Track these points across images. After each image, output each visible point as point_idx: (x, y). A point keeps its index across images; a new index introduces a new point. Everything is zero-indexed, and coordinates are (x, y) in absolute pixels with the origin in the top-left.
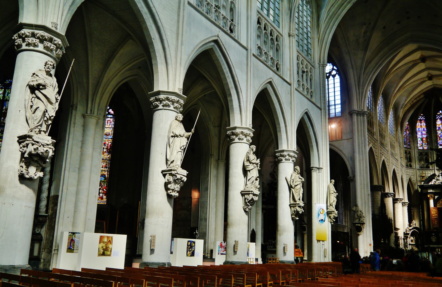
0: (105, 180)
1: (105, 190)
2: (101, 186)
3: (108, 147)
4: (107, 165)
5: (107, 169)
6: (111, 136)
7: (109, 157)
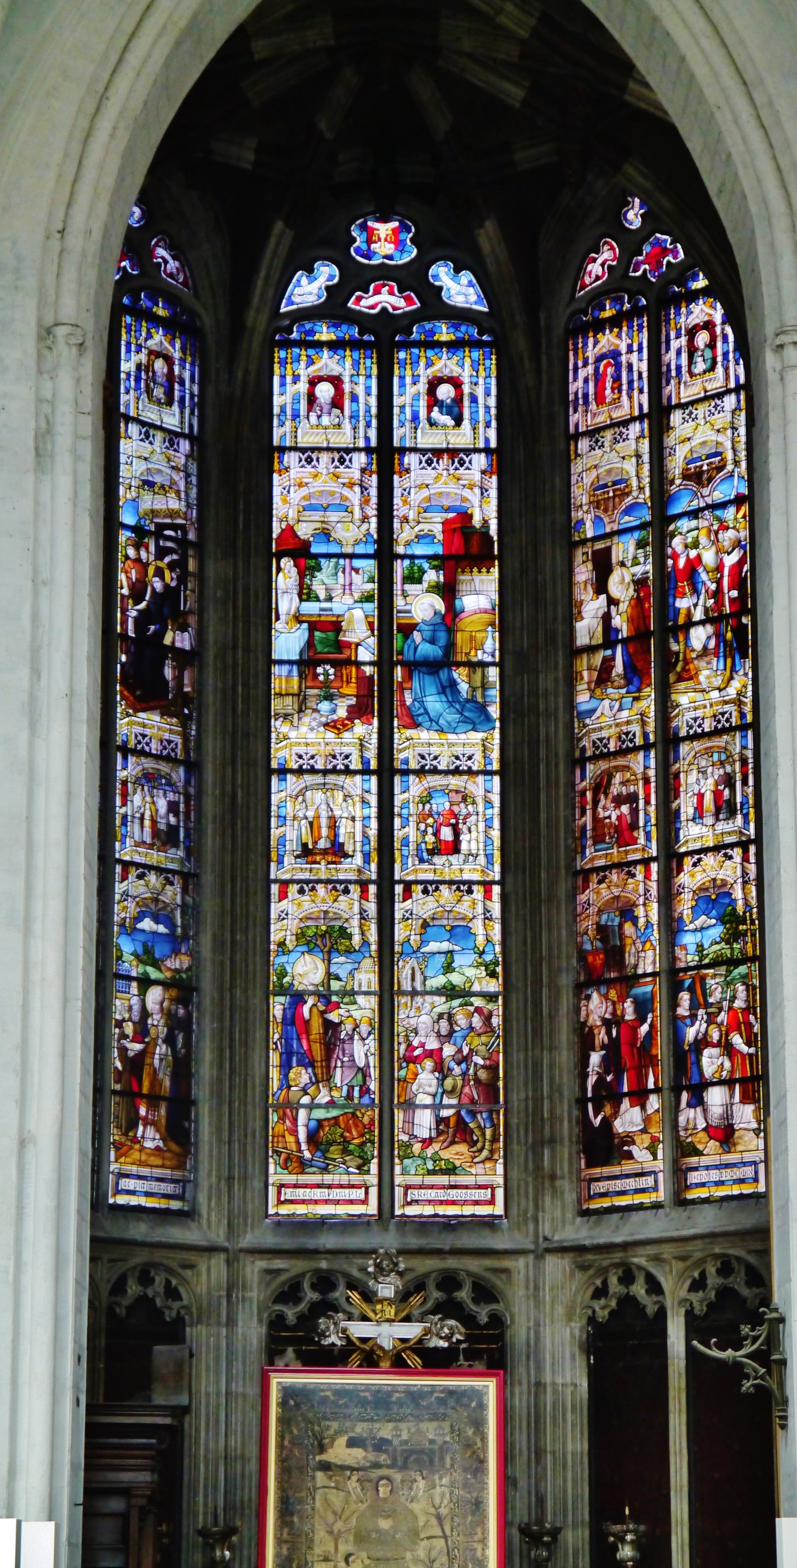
0: (732, 937)
1: (737, 1040)
2: (707, 1005)
3: (717, 594)
4: (729, 780)
5: (739, 818)
6: (732, 476)
7: (738, 702)
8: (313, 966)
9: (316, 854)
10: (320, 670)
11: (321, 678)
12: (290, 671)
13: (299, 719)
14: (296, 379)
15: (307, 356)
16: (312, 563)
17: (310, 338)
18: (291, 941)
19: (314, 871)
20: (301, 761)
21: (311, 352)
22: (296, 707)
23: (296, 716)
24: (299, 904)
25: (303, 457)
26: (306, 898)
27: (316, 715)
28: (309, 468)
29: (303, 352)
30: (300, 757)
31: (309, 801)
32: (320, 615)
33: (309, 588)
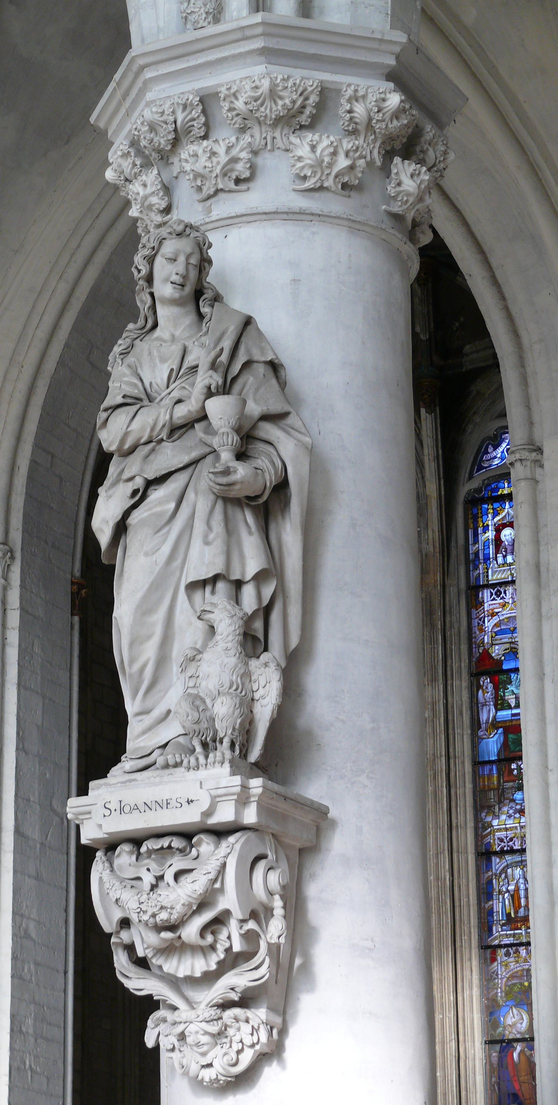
8: (519, 1017)
9: (517, 922)
10: (514, 766)
11: (515, 772)
12: (491, 770)
13: (500, 809)
14: (486, 529)
15: (493, 509)
16: (503, 677)
17: (496, 494)
18: (501, 996)
19: (517, 936)
20: (503, 844)
21: (496, 505)
22: (497, 799)
23: (497, 807)
24: (506, 965)
25: (493, 592)
26: (512, 959)
27: (512, 804)
28: (499, 601)
29: (490, 507)
30: (502, 840)
31: (510, 877)
32: (511, 721)
33: (503, 699)
